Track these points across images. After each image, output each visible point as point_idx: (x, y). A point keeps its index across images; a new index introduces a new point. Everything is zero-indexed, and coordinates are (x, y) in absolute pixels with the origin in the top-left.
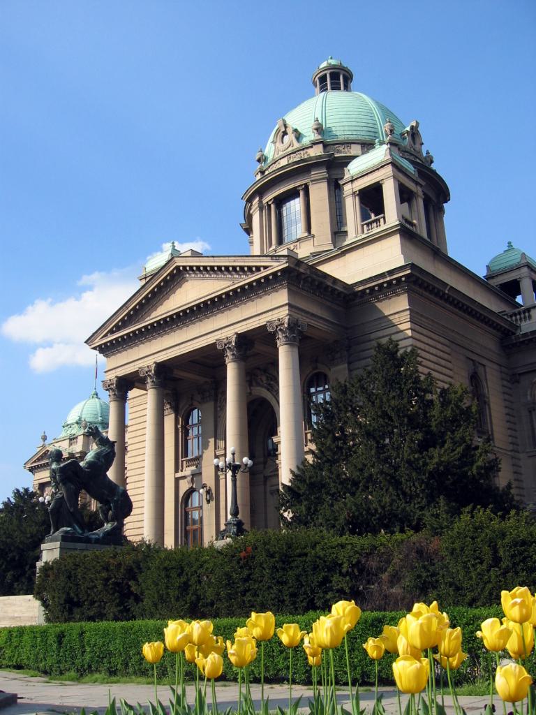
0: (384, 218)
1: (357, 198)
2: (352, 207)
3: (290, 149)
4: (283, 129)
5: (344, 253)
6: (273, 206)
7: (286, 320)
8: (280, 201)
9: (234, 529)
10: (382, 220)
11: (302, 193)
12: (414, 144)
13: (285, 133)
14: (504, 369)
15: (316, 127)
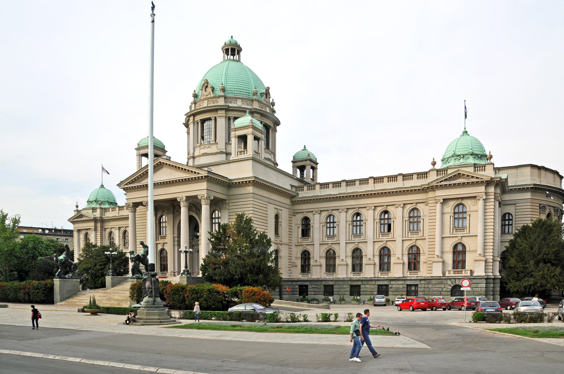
0: (247, 151)
1: (237, 139)
2: (234, 141)
3: (209, 96)
4: (206, 85)
5: (229, 163)
6: (199, 124)
7: (206, 195)
8: (203, 121)
9: (186, 273)
10: (246, 151)
11: (213, 121)
12: (266, 98)
13: (207, 87)
14: (291, 211)
15: (221, 88)
